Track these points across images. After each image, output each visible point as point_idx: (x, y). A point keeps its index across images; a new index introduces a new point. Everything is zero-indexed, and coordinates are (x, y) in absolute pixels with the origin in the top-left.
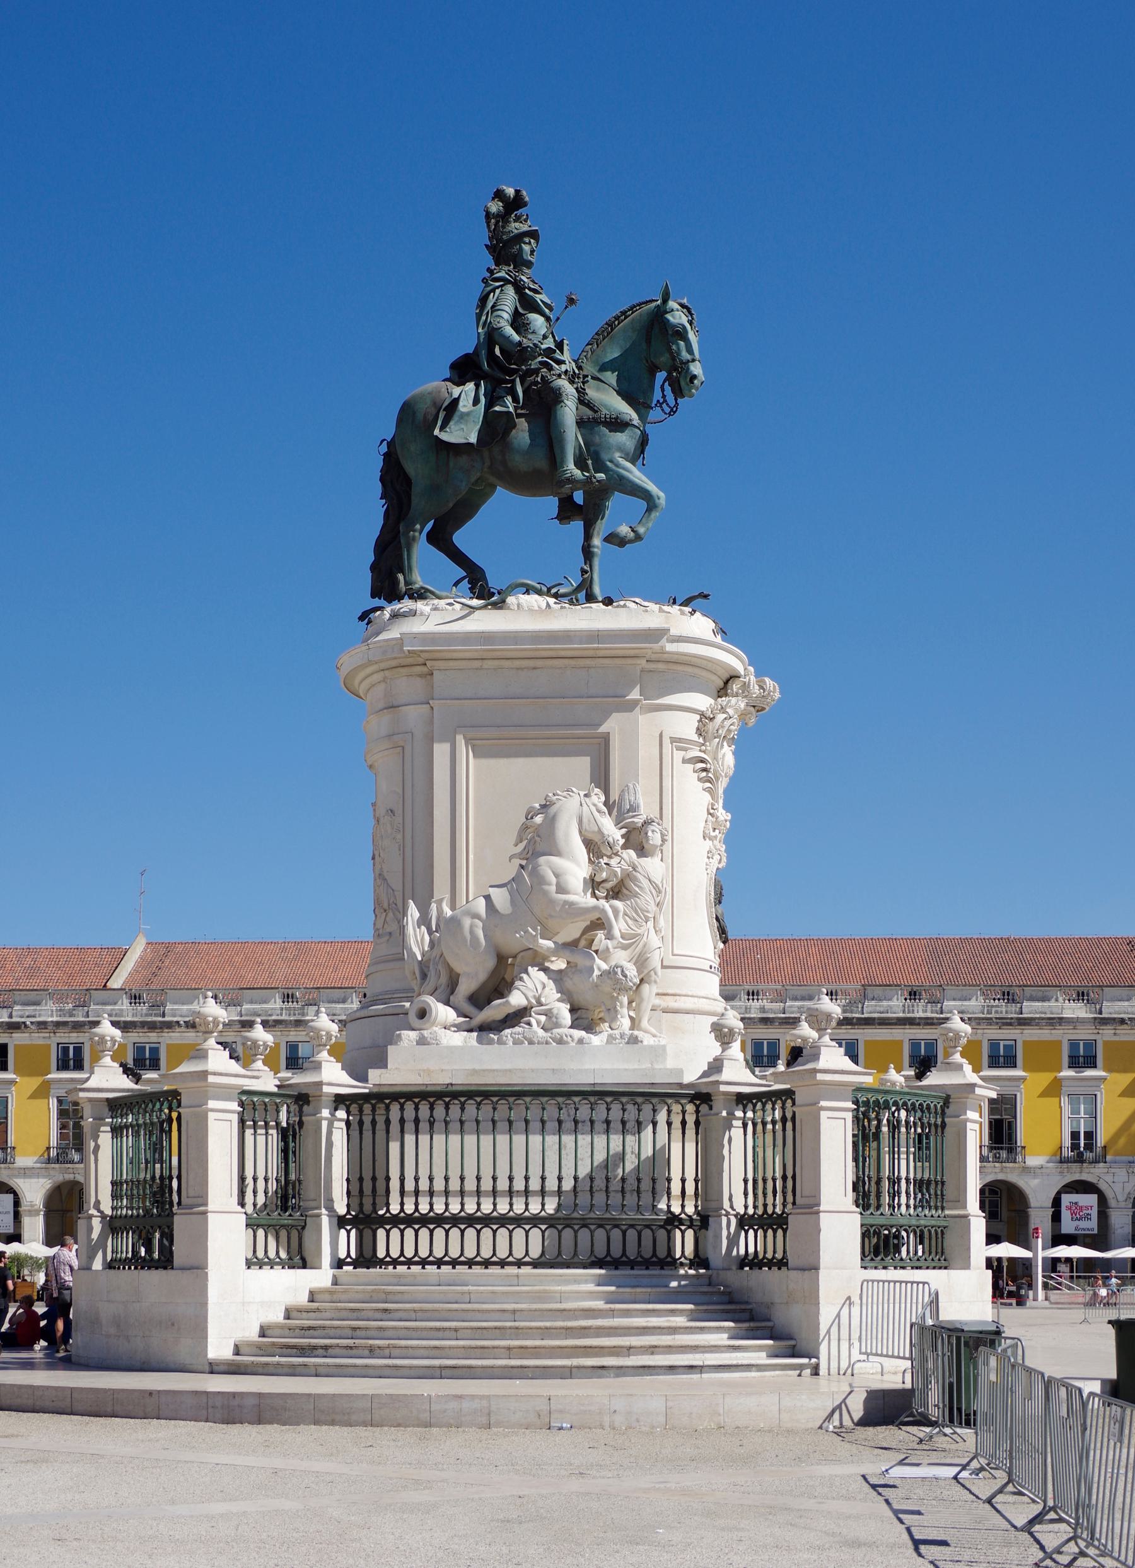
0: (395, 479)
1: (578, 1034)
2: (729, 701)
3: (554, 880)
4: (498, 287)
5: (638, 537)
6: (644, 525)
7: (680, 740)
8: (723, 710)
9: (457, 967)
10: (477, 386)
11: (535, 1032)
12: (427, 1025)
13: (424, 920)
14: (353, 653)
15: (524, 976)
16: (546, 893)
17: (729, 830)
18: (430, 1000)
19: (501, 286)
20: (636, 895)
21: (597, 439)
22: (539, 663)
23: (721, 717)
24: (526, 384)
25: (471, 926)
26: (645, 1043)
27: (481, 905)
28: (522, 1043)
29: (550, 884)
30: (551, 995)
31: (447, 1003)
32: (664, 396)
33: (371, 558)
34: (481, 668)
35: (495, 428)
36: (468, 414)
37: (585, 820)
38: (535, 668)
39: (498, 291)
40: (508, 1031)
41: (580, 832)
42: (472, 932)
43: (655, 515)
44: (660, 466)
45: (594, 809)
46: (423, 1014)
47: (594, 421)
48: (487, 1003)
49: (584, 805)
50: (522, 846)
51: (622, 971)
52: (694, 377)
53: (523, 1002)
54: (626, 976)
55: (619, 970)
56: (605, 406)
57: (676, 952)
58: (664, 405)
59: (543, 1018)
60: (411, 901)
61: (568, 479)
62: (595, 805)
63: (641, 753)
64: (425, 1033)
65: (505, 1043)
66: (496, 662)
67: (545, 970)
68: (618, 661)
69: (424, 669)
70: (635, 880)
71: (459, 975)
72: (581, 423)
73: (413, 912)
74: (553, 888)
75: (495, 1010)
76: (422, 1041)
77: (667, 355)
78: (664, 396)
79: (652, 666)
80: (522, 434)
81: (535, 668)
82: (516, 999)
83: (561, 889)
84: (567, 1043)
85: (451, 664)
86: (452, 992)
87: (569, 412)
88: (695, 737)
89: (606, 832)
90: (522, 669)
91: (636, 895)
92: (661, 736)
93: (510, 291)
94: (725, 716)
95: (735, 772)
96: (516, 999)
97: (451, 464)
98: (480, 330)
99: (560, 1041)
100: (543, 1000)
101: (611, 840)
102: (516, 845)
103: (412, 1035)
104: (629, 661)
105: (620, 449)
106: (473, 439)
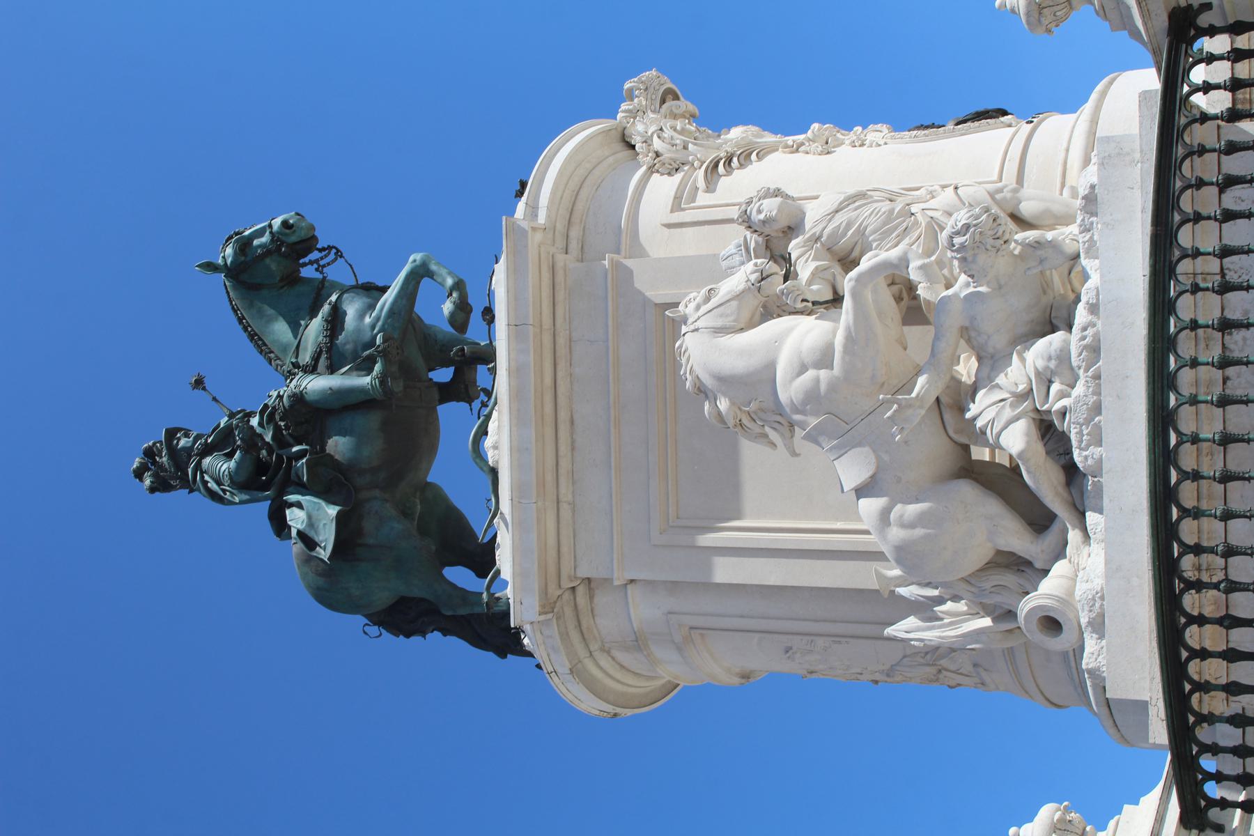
0: (404, 617)
1: (1081, 315)
2: (639, 134)
3: (811, 373)
4: (202, 477)
5: (459, 286)
6: (444, 280)
7: (678, 198)
8: (647, 141)
9: (980, 554)
10: (291, 505)
12: (1071, 616)
13: (925, 610)
14: (570, 696)
15: (979, 423)
16: (833, 387)
17: (836, 124)
18: (1026, 606)
19: (202, 473)
20: (861, 232)
21: (349, 347)
22: (563, 415)
23: (657, 144)
24: (291, 441)
25: (903, 526)
26: (1095, 180)
27: (870, 506)
28: (1098, 427)
29: (817, 381)
30: (1021, 369)
32: (311, 263)
33: (491, 656)
34: (573, 505)
35: (331, 481)
36: (309, 517)
38: (572, 422)
39: (207, 478)
40: (1077, 457)
41: (742, 330)
42: (911, 525)
43: (433, 267)
44: (379, 265)
45: (704, 309)
46: (1052, 624)
47: (331, 356)
48: (1037, 499)
49: (699, 324)
50: (773, 435)
51: (958, 233)
52: (285, 224)
53: (1021, 426)
54: (967, 227)
55: (958, 240)
56: (317, 337)
57: (995, 177)
58: (322, 263)
59: (1055, 388)
60: (890, 631)
61: (381, 383)
62: (698, 308)
63: (691, 253)
64: (1084, 621)
65: (1100, 461)
66: (563, 480)
67: (974, 389)
68: (560, 296)
69: (581, 591)
70: (835, 235)
71: (999, 553)
72: (332, 369)
73: (907, 628)
74: (823, 374)
75: (1043, 480)
76: (1098, 625)
77: (268, 261)
78: (311, 263)
79: (574, 246)
80: (338, 445)
81: (572, 422)
82: (1015, 439)
83: (824, 359)
84: (1097, 338)
85: (564, 549)
86: (1029, 564)
87: (316, 384)
88: (678, 177)
89: (741, 287)
90: (573, 442)
91: (861, 232)
92: (669, 226)
93: (207, 461)
95: (754, 124)
96: (1015, 439)
97: (371, 541)
98: (237, 500)
99: (1094, 350)
100: (1022, 387)
101: (754, 277)
102: (773, 445)
103: (1091, 644)
104: (560, 277)
105: (361, 316)
106: (333, 511)
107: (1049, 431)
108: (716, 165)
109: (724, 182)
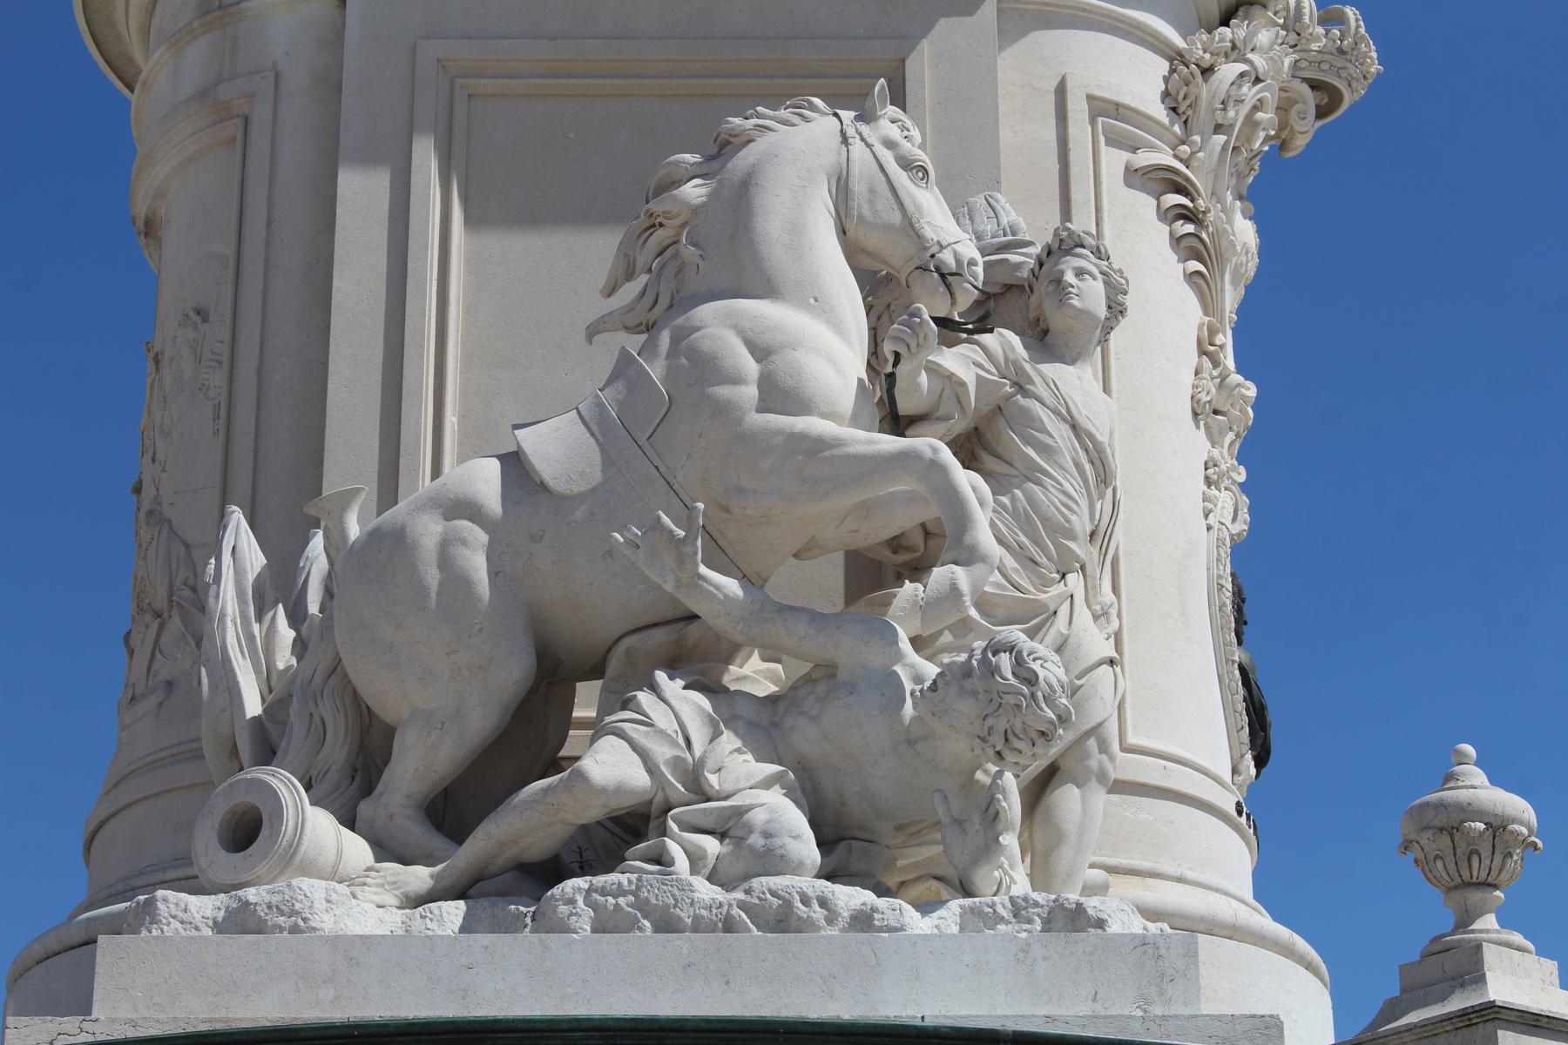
2: (1251, 35)
3: (750, 367)
8: (1235, 51)
9: (389, 694)
11: (687, 888)
12: (261, 870)
13: (279, 587)
15: (644, 697)
16: (725, 412)
17: (1252, 431)
18: (285, 785)
20: (1032, 474)
23: (1229, 71)
25: (445, 545)
26: (1114, 928)
27: (484, 479)
28: (631, 926)
29: (737, 380)
31: (350, 822)
37: (858, 187)
40: (575, 885)
41: (842, 232)
42: (445, 561)
45: (887, 157)
46: (245, 831)
49: (857, 147)
50: (631, 290)
51: (1019, 662)
53: (638, 777)
54: (1031, 680)
55: (1005, 661)
57: (1133, 739)
59: (711, 845)
62: (890, 144)
63: (1005, 134)
64: (251, 894)
65: (564, 928)
67: (710, 687)
70: (1027, 423)
71: (390, 732)
73: (243, 551)
74: (749, 392)
75: (529, 818)
76: (240, 922)
82: (611, 766)
83: (780, 394)
84: (805, 926)
86: (368, 790)
88: (1160, 113)
89: (929, 233)
91: (1032, 474)
92: (1061, 91)
94: (1243, 67)
95: (1259, 268)
96: (611, 766)
99: (781, 920)
101: (947, 257)
102: (611, 291)
103: (204, 907)
107: (627, 831)
108: (1180, 190)
109: (1144, 204)
